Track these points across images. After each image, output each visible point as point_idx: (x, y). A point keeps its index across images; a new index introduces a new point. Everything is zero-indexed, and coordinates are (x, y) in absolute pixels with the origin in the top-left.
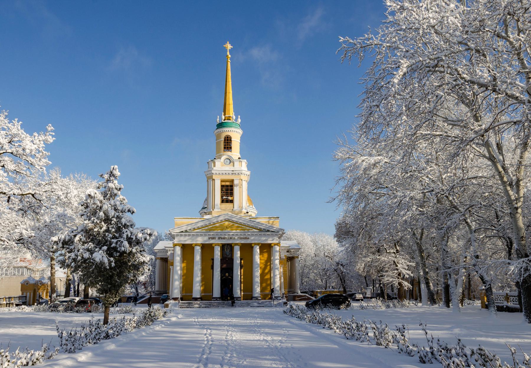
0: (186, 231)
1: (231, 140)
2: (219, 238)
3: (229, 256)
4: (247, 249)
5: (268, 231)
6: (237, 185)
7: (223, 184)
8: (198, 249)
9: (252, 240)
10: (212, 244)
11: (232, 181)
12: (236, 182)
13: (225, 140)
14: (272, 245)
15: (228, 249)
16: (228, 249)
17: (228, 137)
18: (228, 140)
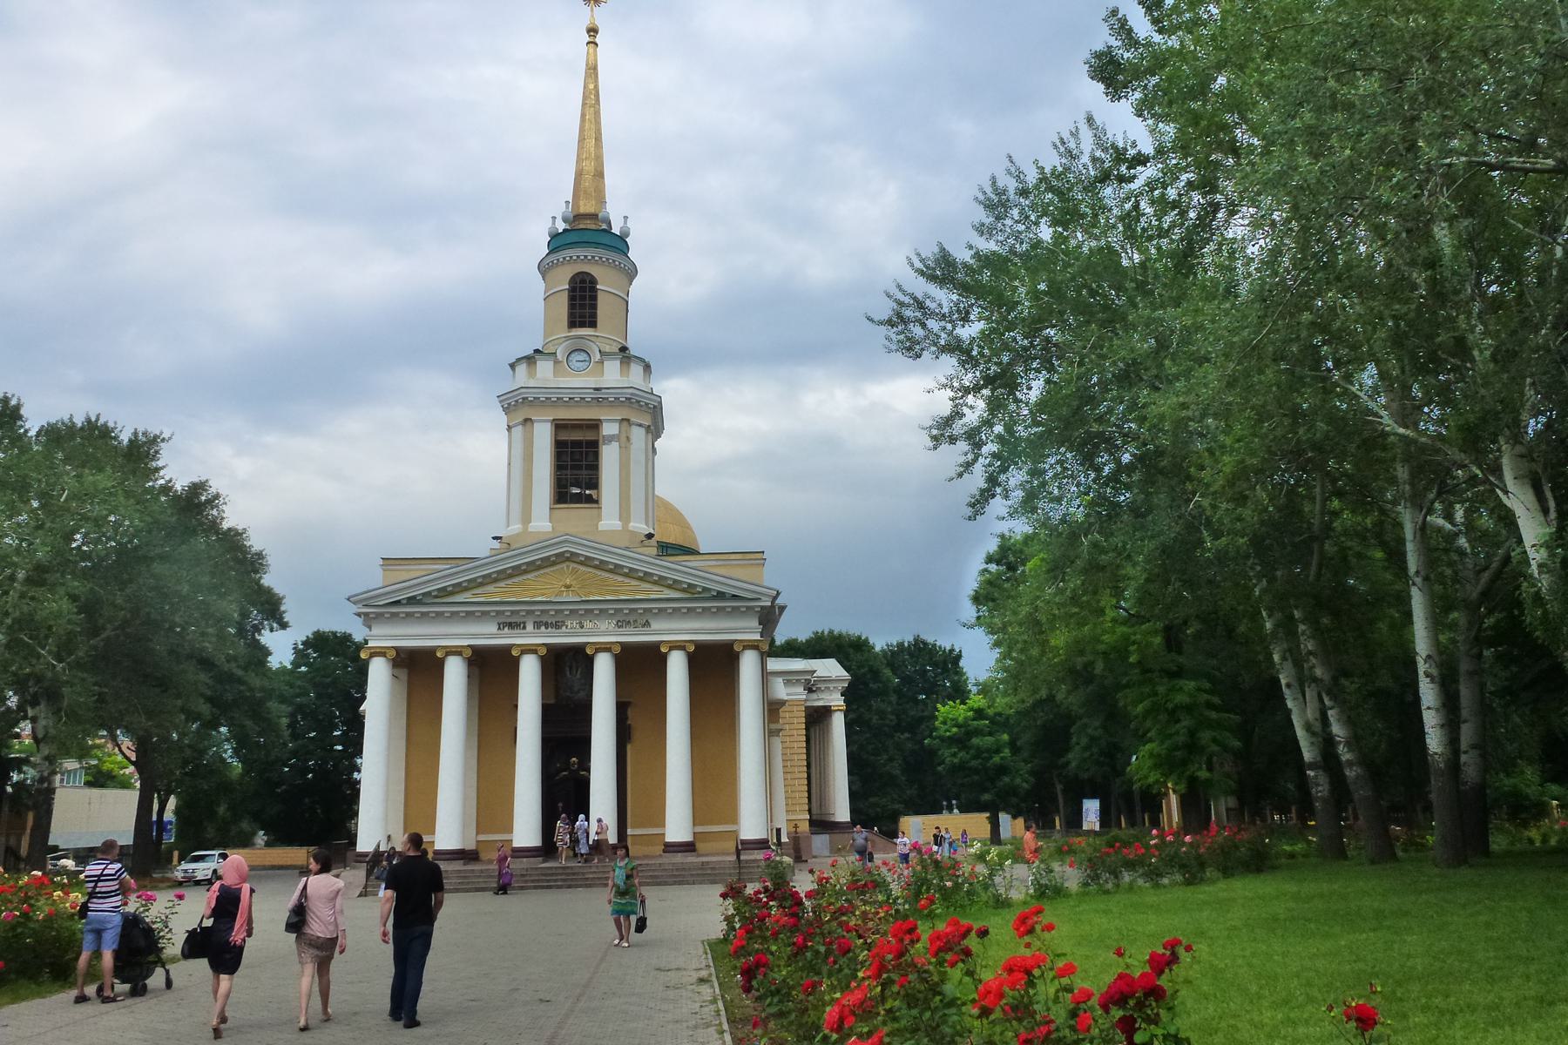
0: (412, 601)
1: (594, 290)
2: (537, 625)
3: (582, 694)
4: (640, 666)
5: (721, 596)
6: (611, 439)
7: (564, 437)
8: (455, 674)
9: (661, 631)
10: (509, 648)
11: (595, 425)
12: (609, 429)
13: (572, 290)
14: (737, 648)
15: (566, 670)
16: (566, 670)
17: (583, 281)
18: (583, 289)
